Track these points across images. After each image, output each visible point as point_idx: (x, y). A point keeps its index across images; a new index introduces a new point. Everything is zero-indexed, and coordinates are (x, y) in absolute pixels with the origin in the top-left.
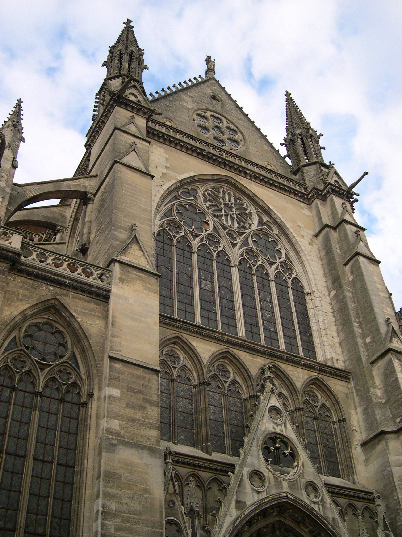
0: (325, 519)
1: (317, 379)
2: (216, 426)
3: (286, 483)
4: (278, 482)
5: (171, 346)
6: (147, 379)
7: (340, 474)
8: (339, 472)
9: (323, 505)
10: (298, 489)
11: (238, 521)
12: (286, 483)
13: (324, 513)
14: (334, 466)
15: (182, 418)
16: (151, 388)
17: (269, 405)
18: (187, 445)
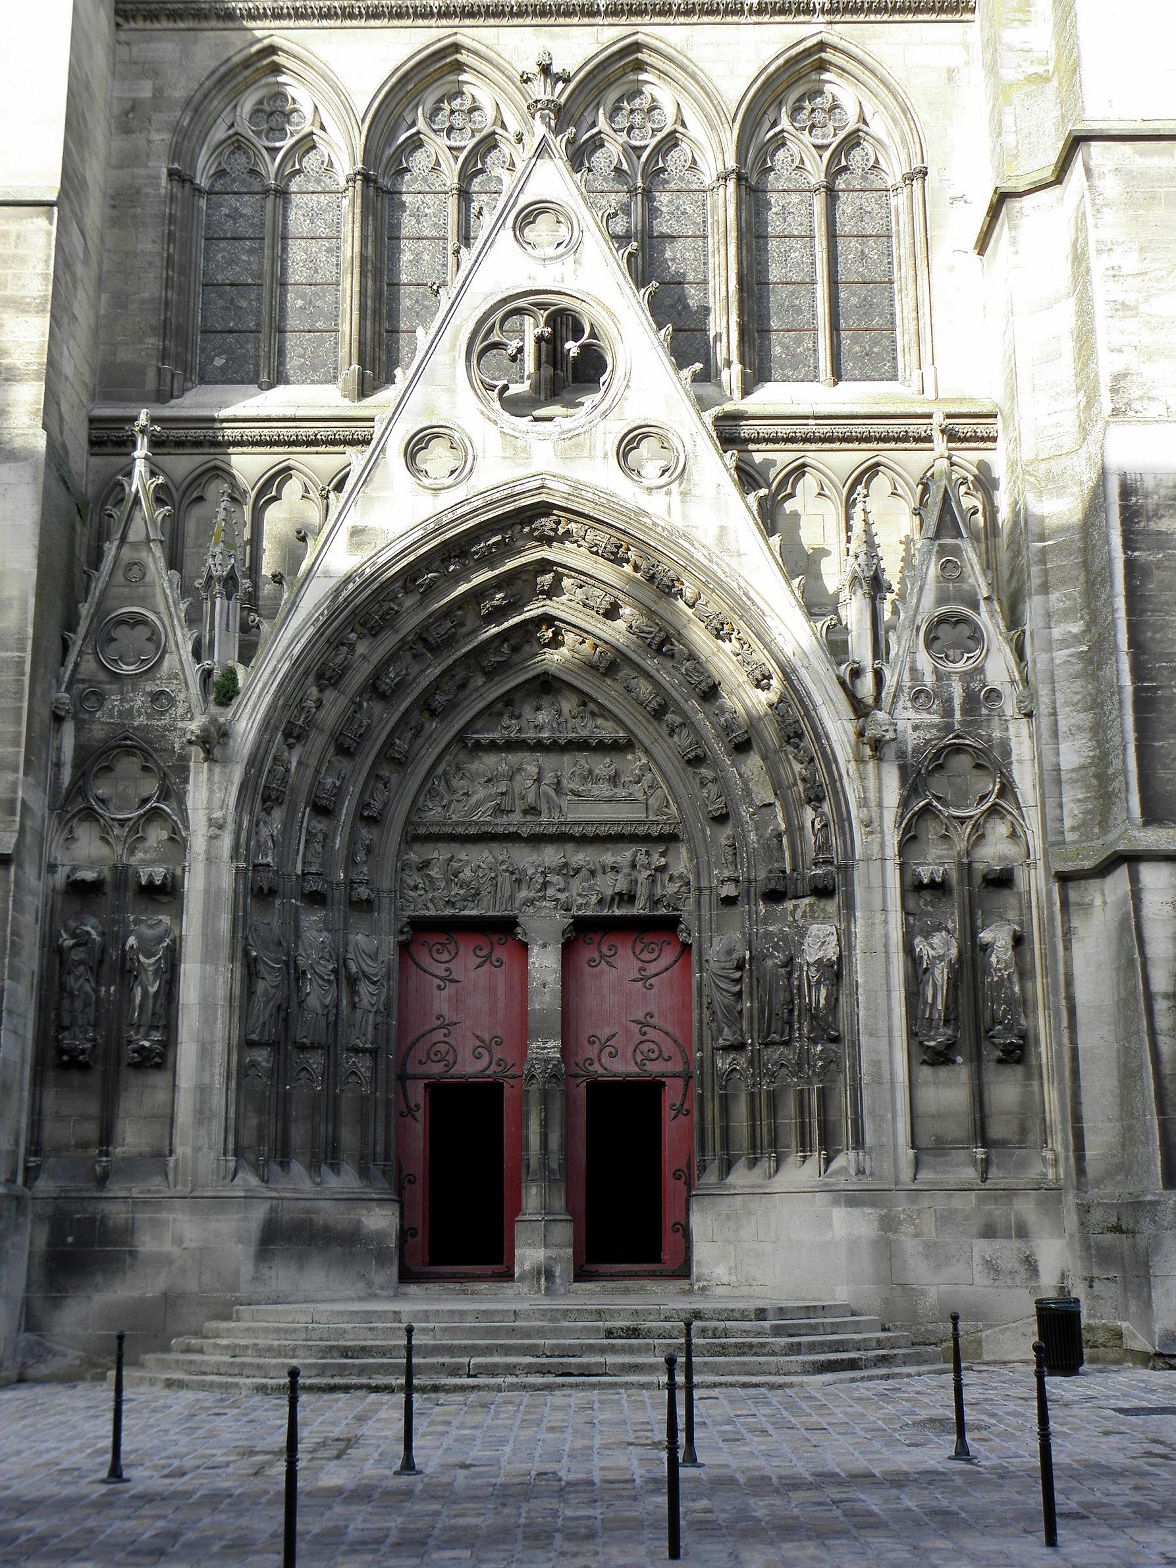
0: (687, 539)
1: (822, 46)
2: (417, 301)
3: (549, 445)
4: (515, 447)
5: (263, 81)
6: (13, 238)
7: (895, 368)
8: (894, 359)
9: (684, 494)
10: (591, 457)
11: (351, 586)
12: (549, 445)
13: (685, 516)
14: (876, 344)
15: (300, 303)
16: (23, 260)
17: (523, 201)
18: (313, 382)
